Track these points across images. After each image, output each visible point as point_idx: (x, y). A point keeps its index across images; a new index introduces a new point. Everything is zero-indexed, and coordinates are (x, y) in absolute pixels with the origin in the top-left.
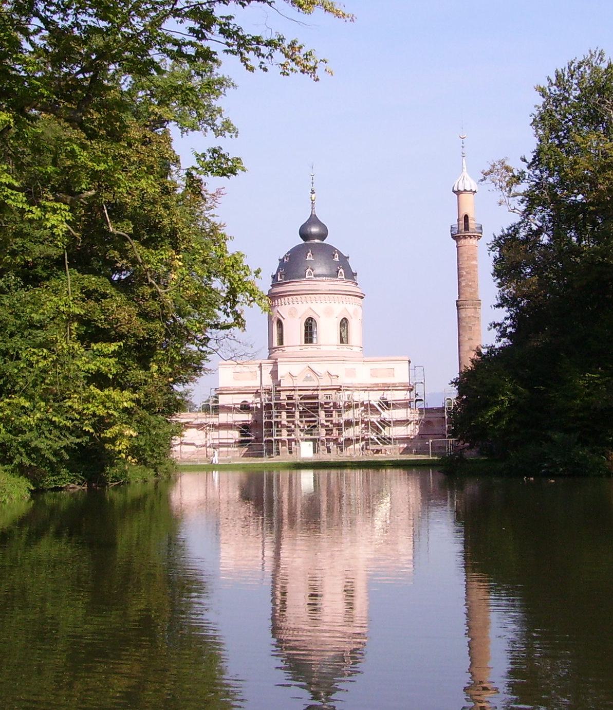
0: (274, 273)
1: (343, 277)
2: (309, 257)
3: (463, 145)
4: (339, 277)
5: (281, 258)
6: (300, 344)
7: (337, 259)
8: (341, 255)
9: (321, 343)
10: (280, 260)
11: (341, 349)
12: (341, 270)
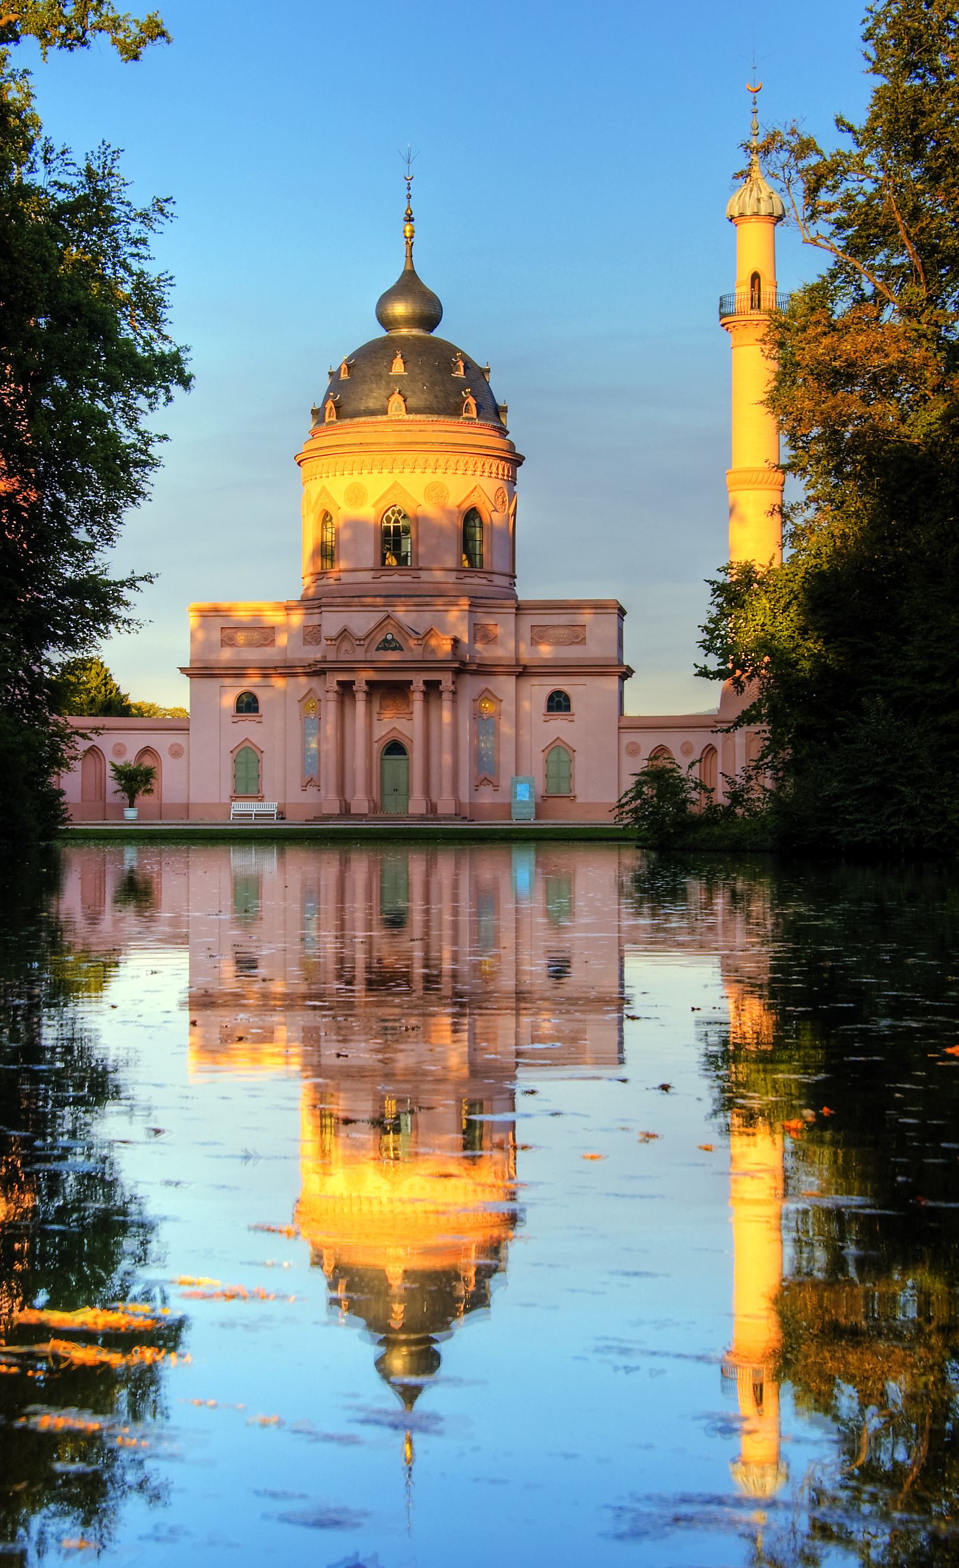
0: (319, 406)
1: (474, 415)
2: (398, 367)
3: (757, 107)
4: (465, 415)
5: (335, 369)
6: (371, 565)
7: (460, 373)
8: (469, 365)
9: (421, 565)
10: (331, 374)
11: (468, 580)
12: (471, 401)
